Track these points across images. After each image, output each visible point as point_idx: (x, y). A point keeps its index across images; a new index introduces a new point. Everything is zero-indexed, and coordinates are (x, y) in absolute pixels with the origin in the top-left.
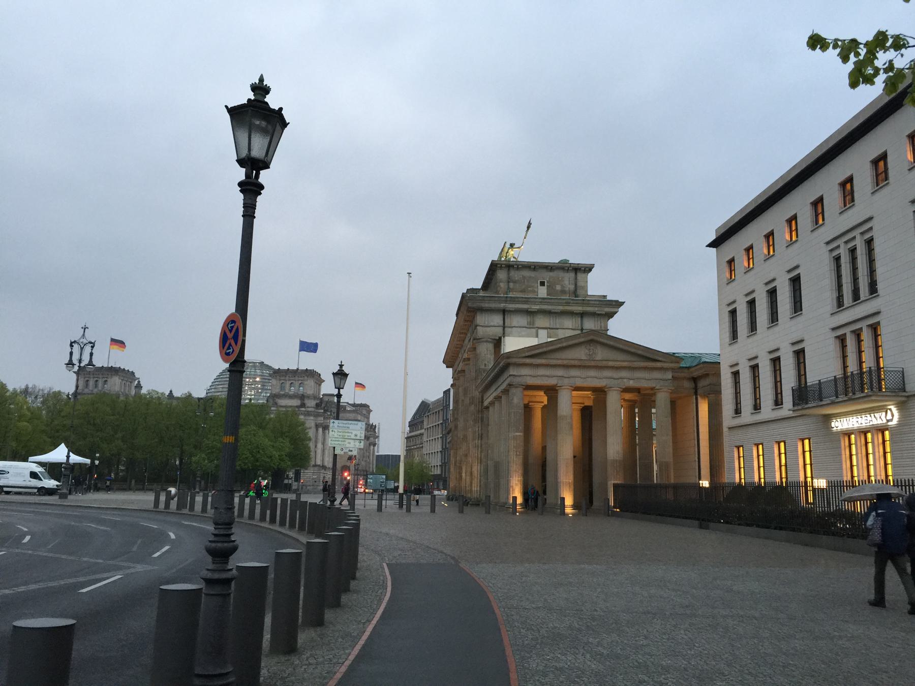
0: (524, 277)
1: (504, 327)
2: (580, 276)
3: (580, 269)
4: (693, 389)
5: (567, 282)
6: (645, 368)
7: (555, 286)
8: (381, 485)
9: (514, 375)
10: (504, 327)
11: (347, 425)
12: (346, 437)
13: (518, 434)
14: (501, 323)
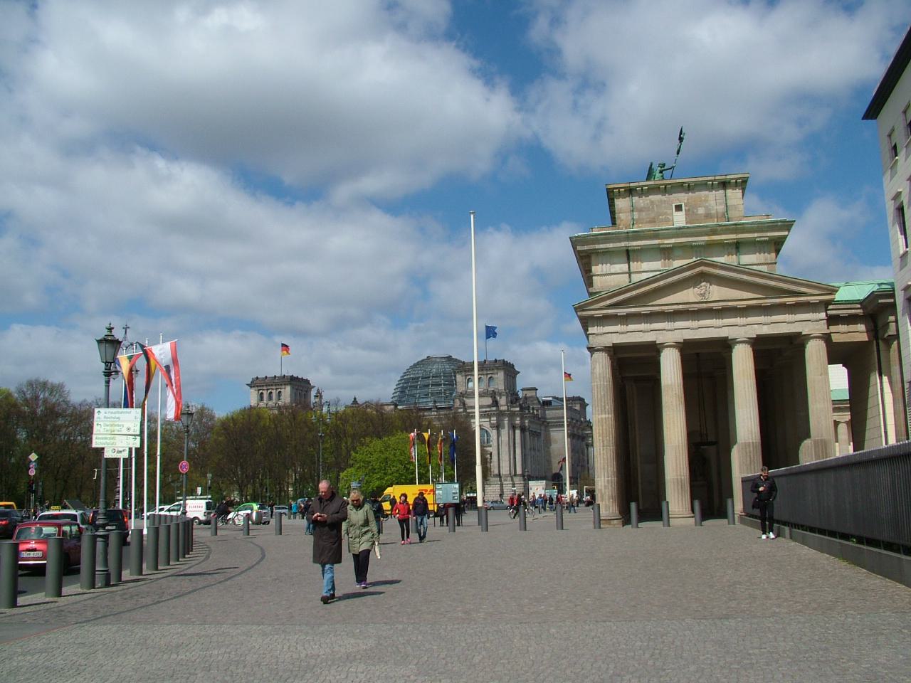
0: (652, 202)
4: (872, 330)
5: (713, 203)
8: (453, 497)
9: (594, 334)
11: (117, 415)
12: (116, 433)
13: (604, 416)
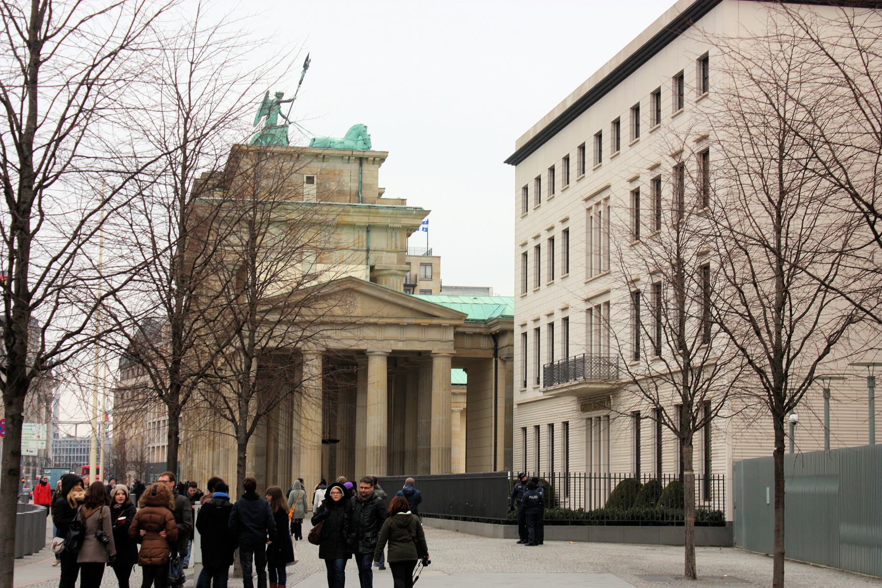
2: (367, 168)
3: (367, 159)
6: (418, 325)
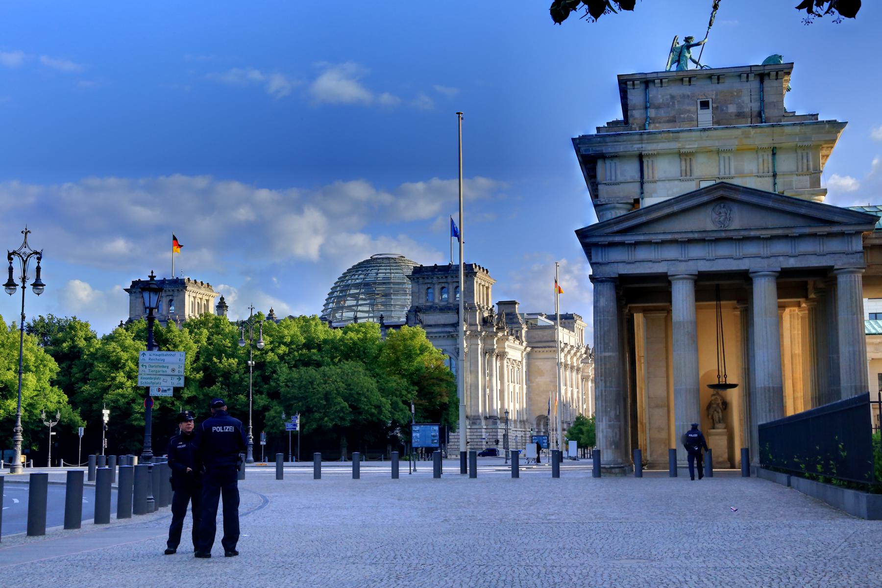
0: (672, 97)
1: (642, 184)
6: (814, 235)
7: (727, 107)
8: (433, 440)
10: (642, 184)
11: (162, 357)
13: (607, 354)
14: (637, 176)
